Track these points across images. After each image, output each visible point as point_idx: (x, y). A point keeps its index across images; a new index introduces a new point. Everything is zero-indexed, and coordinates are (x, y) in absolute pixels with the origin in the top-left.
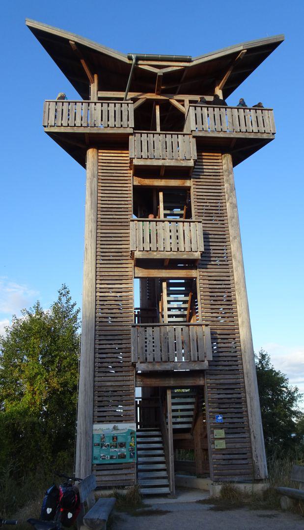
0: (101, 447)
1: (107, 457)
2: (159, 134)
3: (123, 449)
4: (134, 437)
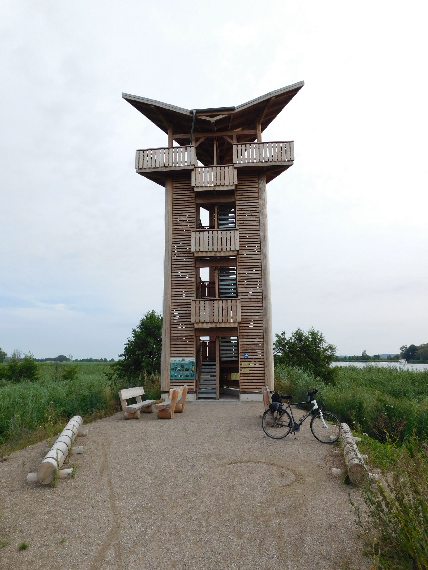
0: (175, 370)
1: (179, 376)
2: (216, 167)
3: (187, 372)
4: (194, 366)
